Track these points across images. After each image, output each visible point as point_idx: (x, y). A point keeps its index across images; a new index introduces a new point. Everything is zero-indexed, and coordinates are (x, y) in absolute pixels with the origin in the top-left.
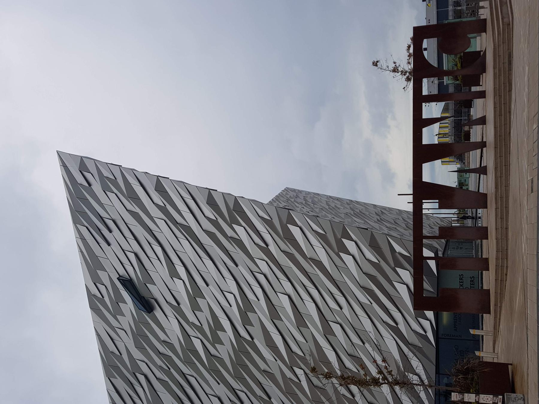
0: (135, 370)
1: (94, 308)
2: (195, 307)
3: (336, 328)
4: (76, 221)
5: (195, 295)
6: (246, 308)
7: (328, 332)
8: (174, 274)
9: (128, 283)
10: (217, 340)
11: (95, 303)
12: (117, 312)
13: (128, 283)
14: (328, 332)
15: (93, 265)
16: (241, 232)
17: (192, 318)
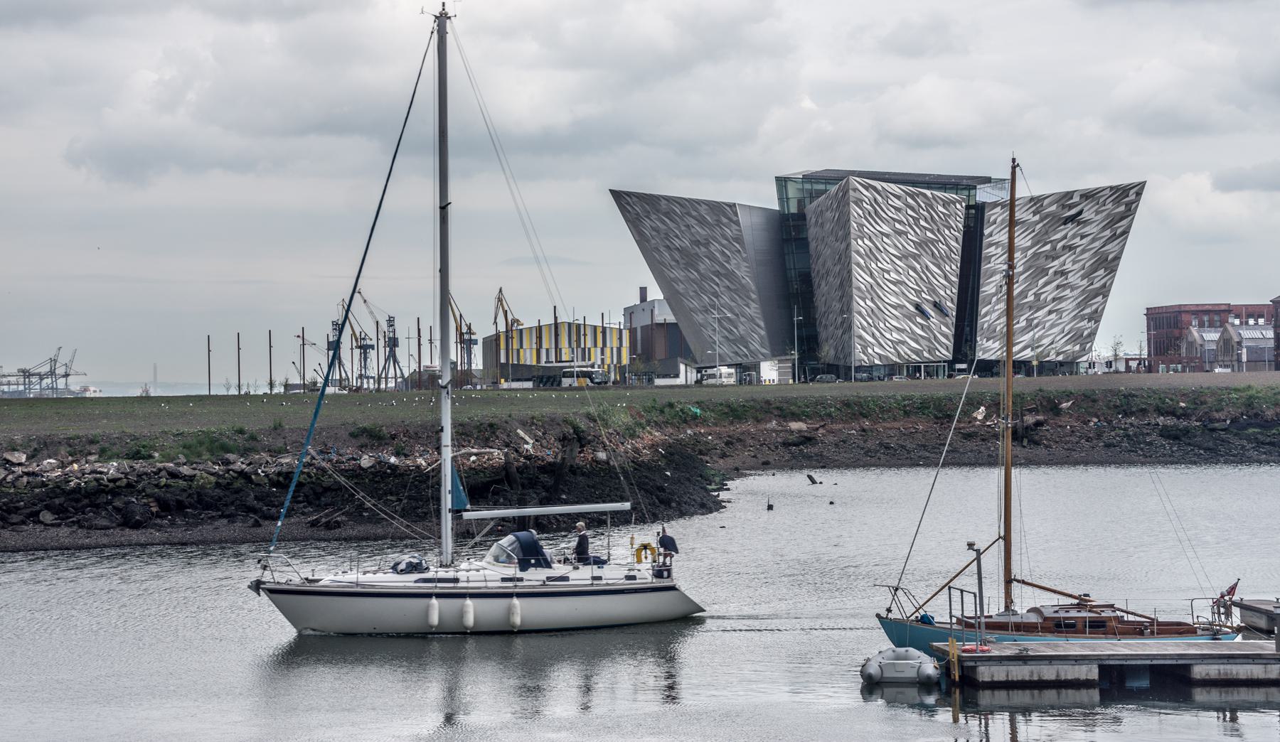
0: (1035, 213)
1: (1068, 193)
2: (1064, 247)
3: (1053, 316)
4: (1111, 188)
5: (1071, 248)
6: (1063, 273)
7: (1050, 312)
8: (1083, 237)
9: (1080, 213)
10: (1047, 257)
11: (1069, 195)
12: (1064, 207)
13: (1080, 213)
14: (1050, 312)
15: (1088, 196)
16: (1101, 272)
17: (1060, 245)
